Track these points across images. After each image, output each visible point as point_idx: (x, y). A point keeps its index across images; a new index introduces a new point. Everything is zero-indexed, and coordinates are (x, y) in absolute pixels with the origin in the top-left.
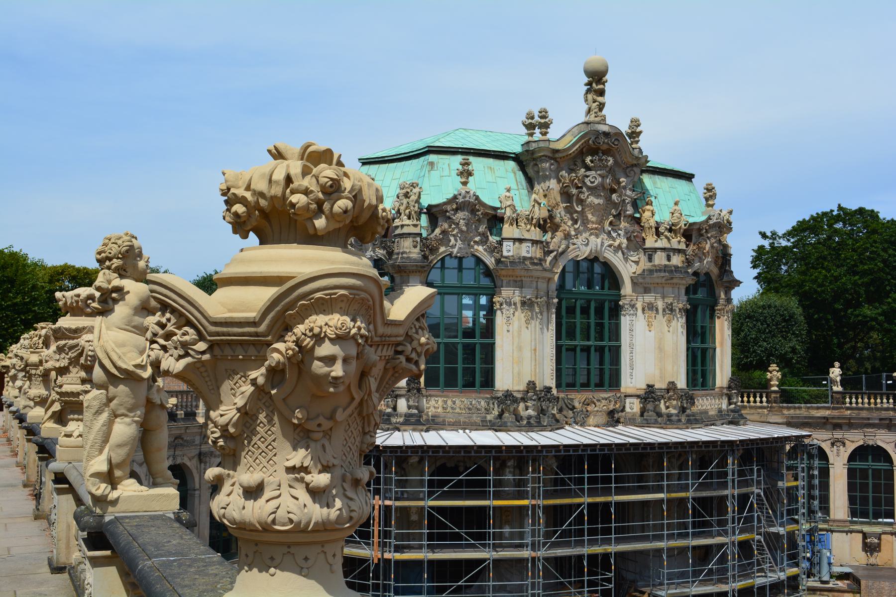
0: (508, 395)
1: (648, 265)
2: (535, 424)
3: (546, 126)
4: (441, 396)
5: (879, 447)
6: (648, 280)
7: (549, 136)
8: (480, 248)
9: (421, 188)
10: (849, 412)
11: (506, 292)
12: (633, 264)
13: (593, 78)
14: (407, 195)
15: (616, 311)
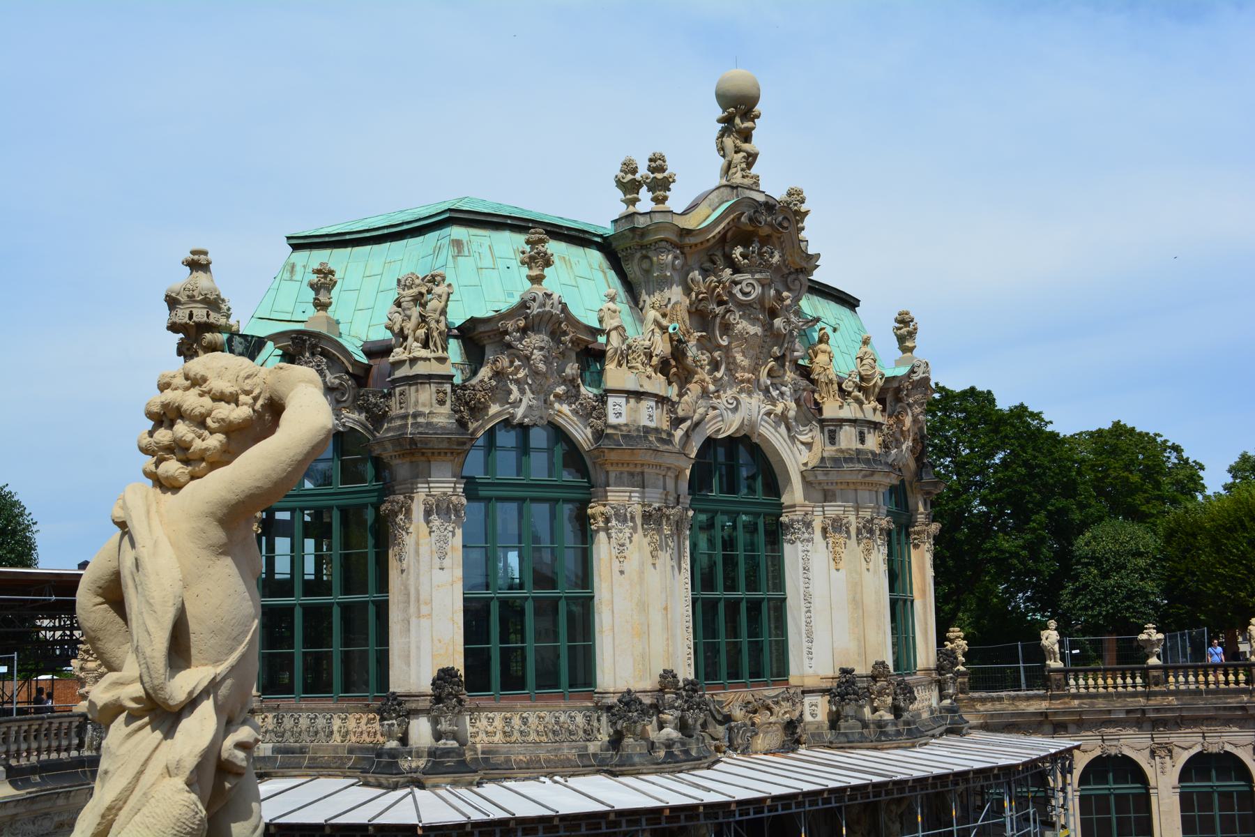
0: (629, 700)
1: (830, 451)
2: (682, 757)
3: (665, 184)
4: (499, 710)
5: (1125, 757)
6: (833, 477)
7: (669, 205)
8: (565, 408)
9: (449, 285)
10: (1076, 702)
11: (620, 496)
12: (802, 447)
13: (736, 108)
14: (419, 299)
15: (776, 533)
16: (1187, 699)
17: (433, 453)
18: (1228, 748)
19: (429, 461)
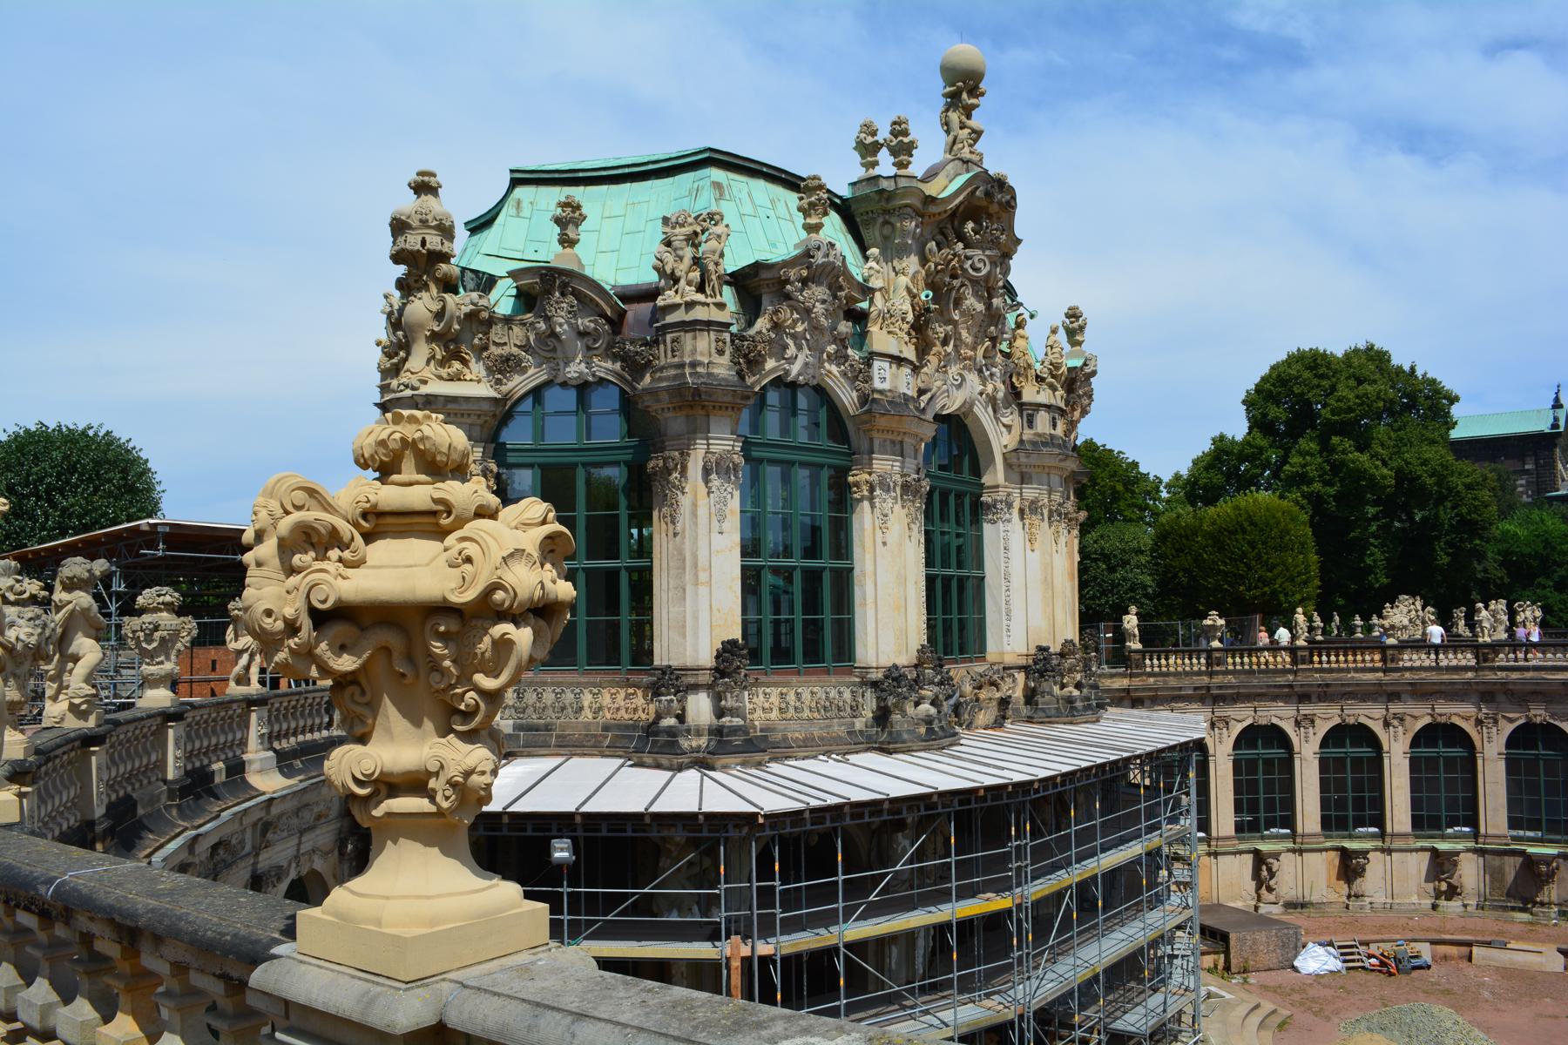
1: (1028, 434)
2: (941, 733)
3: (908, 149)
4: (776, 685)
6: (1034, 460)
7: (912, 170)
8: (834, 369)
9: (727, 226)
10: (1152, 680)
11: (885, 465)
12: (1004, 429)
13: (964, 83)
14: (693, 240)
16: (1243, 677)
17: (714, 407)
18: (1275, 721)
19: (708, 416)
